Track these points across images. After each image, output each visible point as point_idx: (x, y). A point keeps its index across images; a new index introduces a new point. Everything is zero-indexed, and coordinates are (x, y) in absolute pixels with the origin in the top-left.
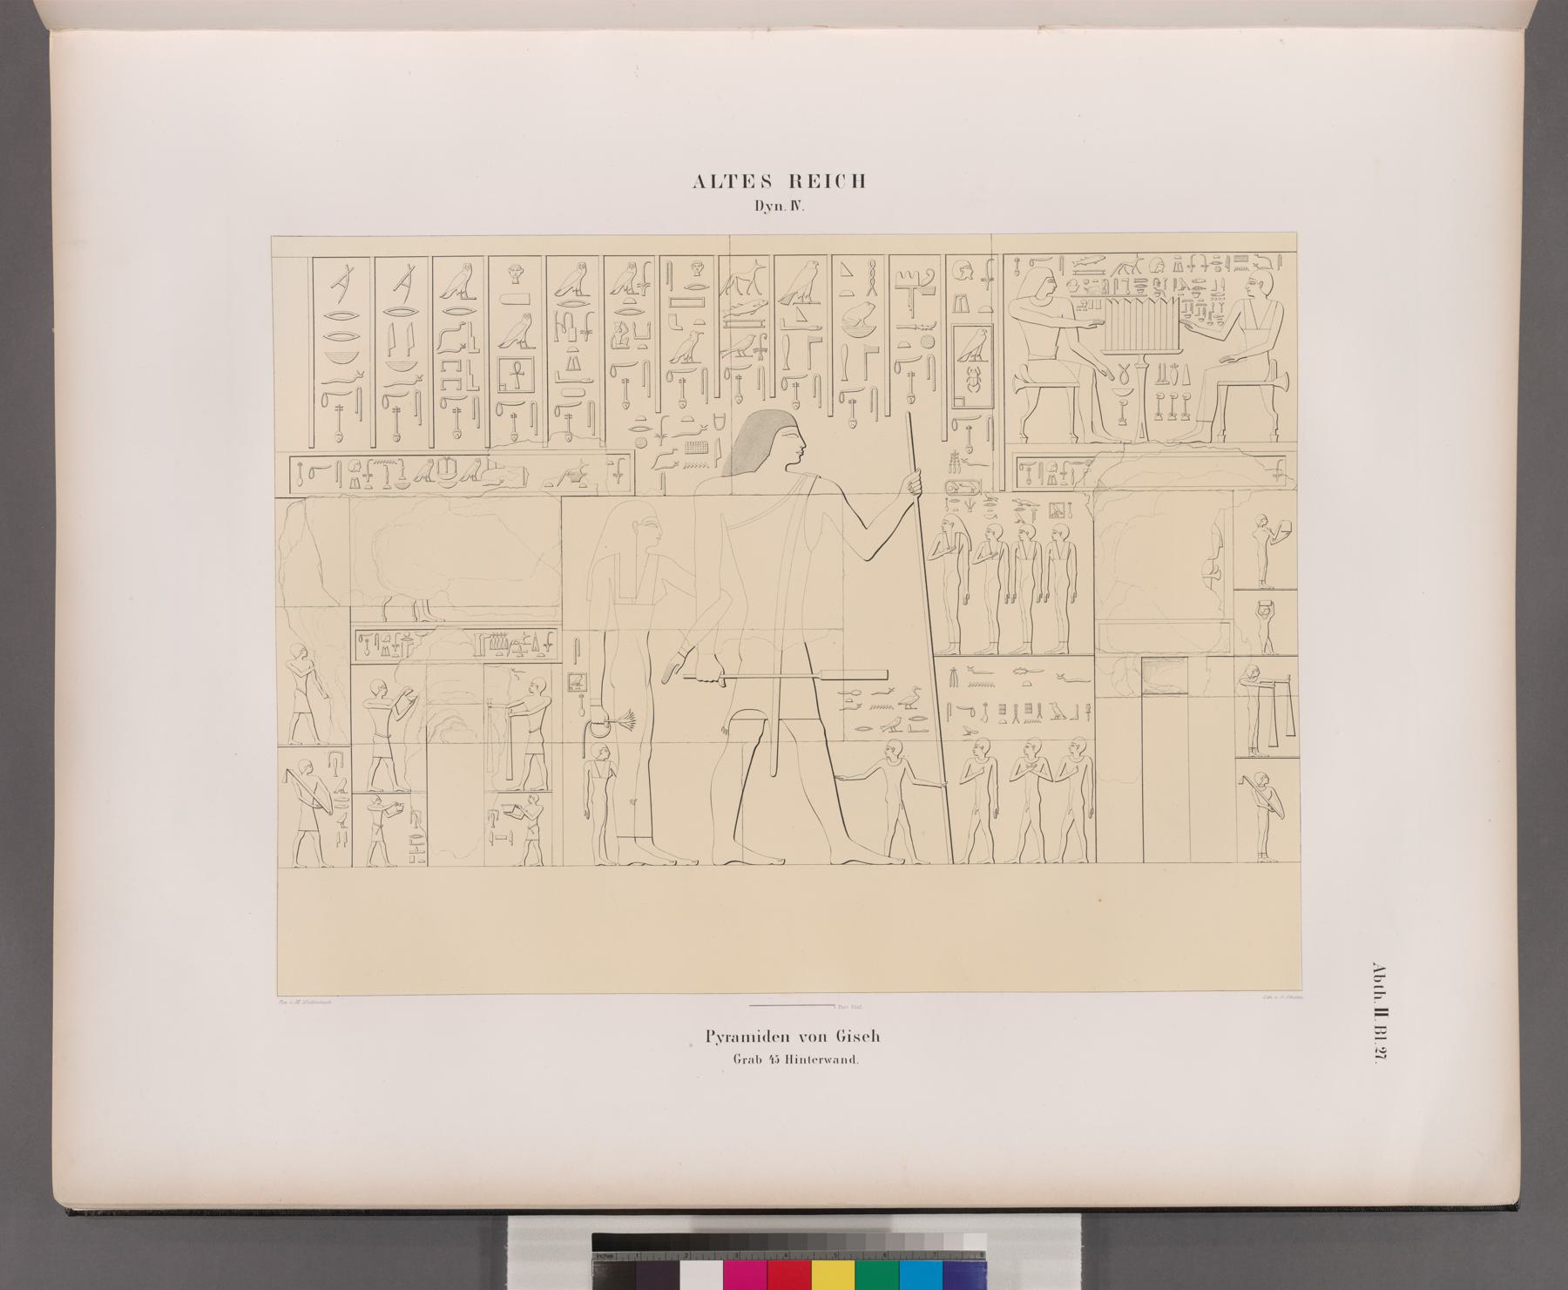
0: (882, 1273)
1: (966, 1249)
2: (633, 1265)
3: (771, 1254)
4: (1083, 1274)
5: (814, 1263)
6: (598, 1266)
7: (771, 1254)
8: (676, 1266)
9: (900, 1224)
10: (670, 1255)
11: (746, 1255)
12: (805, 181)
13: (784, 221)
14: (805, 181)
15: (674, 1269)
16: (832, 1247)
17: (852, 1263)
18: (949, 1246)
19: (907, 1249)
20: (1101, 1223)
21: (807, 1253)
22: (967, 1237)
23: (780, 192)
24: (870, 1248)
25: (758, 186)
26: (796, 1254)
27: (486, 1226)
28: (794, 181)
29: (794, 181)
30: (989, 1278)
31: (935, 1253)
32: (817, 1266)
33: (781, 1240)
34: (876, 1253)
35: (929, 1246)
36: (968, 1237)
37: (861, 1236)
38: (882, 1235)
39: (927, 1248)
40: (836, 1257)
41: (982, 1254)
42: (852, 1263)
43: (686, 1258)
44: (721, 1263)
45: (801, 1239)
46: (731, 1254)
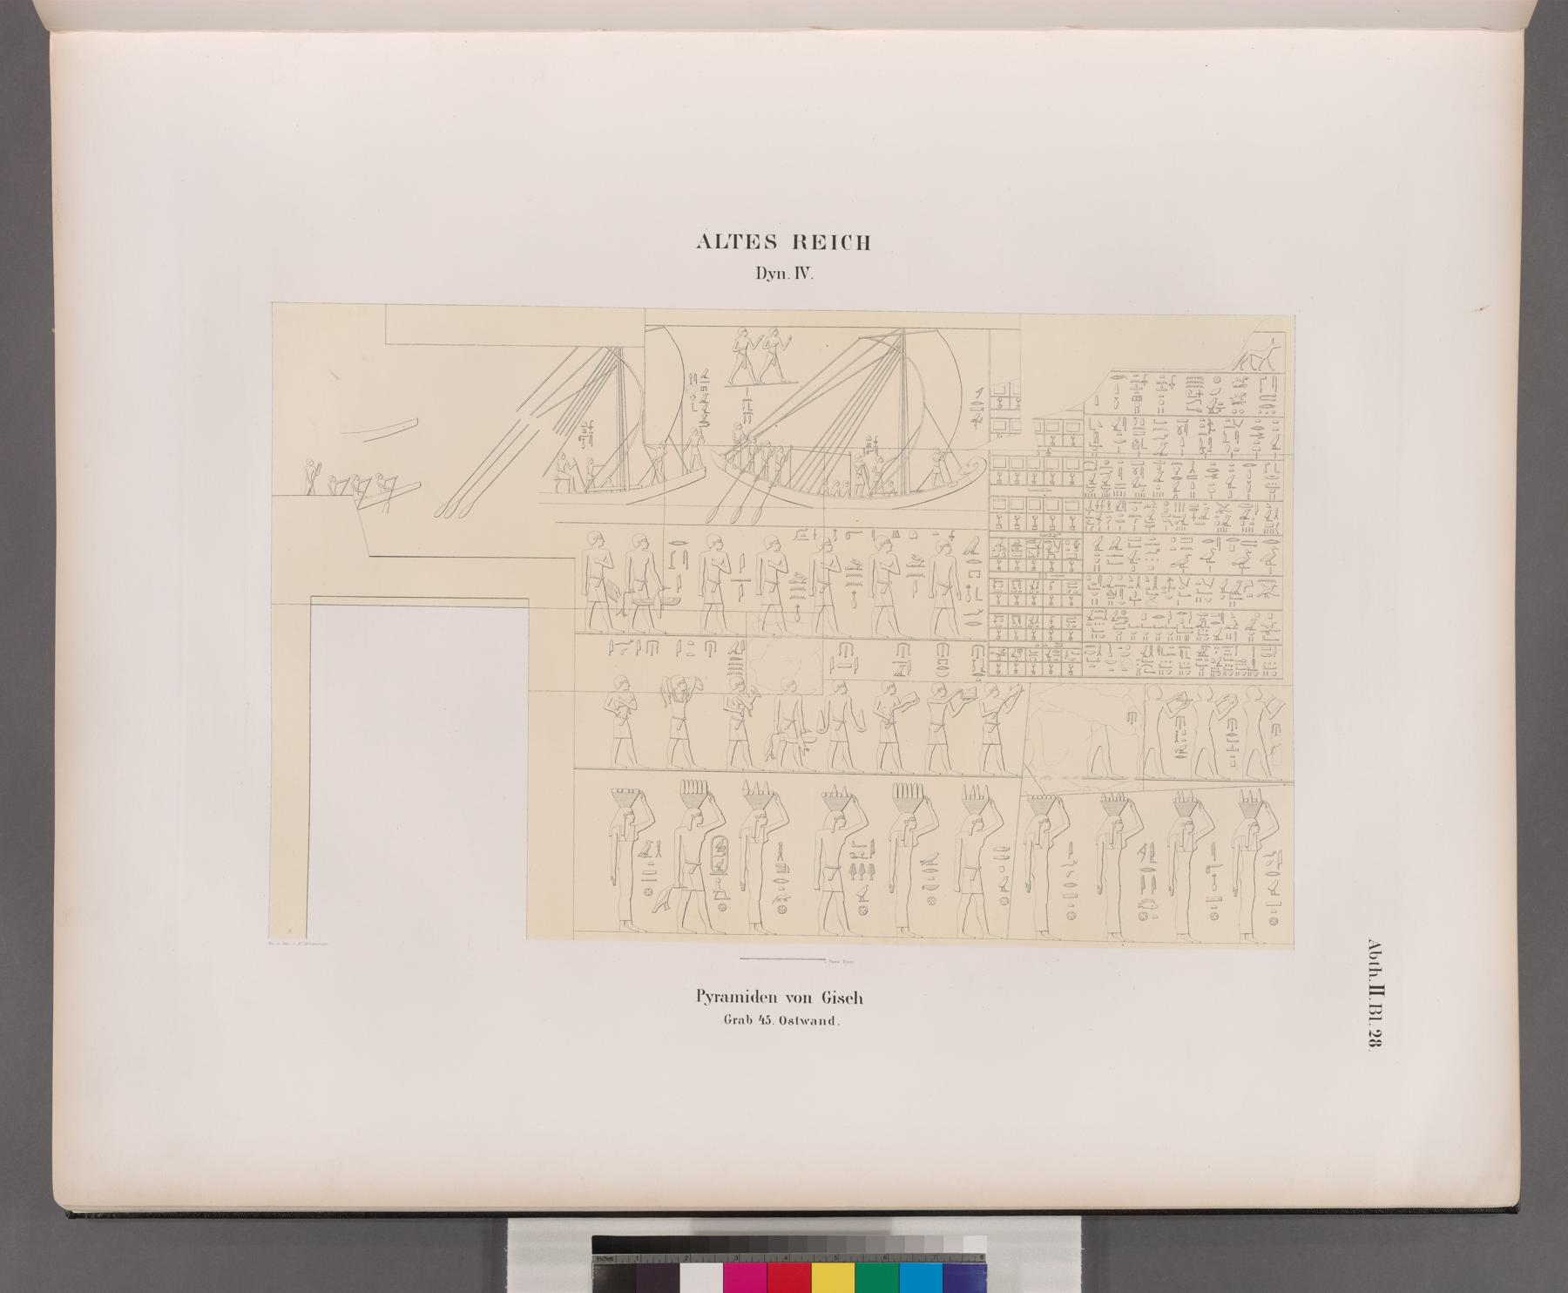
0: (882, 1277)
2: (633, 1267)
4: (1083, 1277)
9: (900, 1226)
10: (669, 1258)
11: (746, 1257)
15: (674, 1271)
16: (832, 1249)
17: (850, 1268)
19: (908, 1250)
20: (1104, 1228)
22: (967, 1239)
24: (871, 1250)
26: (795, 1257)
27: (487, 1228)
30: (989, 1280)
31: (935, 1257)
34: (876, 1256)
36: (968, 1239)
37: (861, 1239)
38: (882, 1237)
39: (928, 1250)
40: (836, 1259)
42: (850, 1268)
45: (801, 1242)
46: (731, 1257)
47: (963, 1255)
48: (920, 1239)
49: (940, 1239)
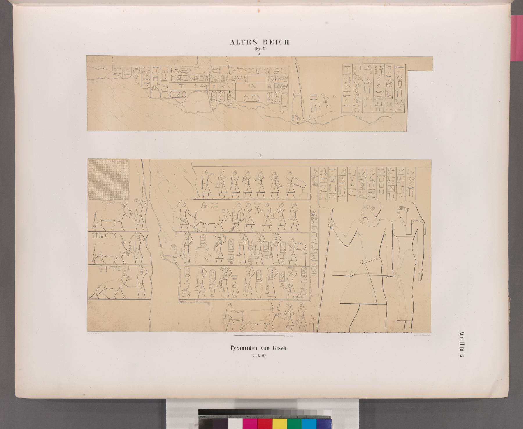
3: (259, 416)
5: (273, 419)
6: (200, 419)
7: (259, 416)
8: (227, 419)
10: (225, 417)
11: (250, 417)
12: (268, 42)
13: (263, 53)
14: (268, 42)
17: (285, 420)
18: (319, 414)
19: (305, 415)
21: (271, 416)
23: (260, 45)
24: (292, 414)
25: (252, 44)
26: (267, 417)
28: (265, 42)
29: (265, 42)
32: (274, 420)
34: (294, 416)
35: (311, 415)
37: (289, 411)
38: (296, 410)
40: (281, 417)
41: (330, 417)
42: (285, 420)
43: (230, 418)
44: (241, 419)
46: (245, 416)
48: (309, 411)
49: (316, 411)
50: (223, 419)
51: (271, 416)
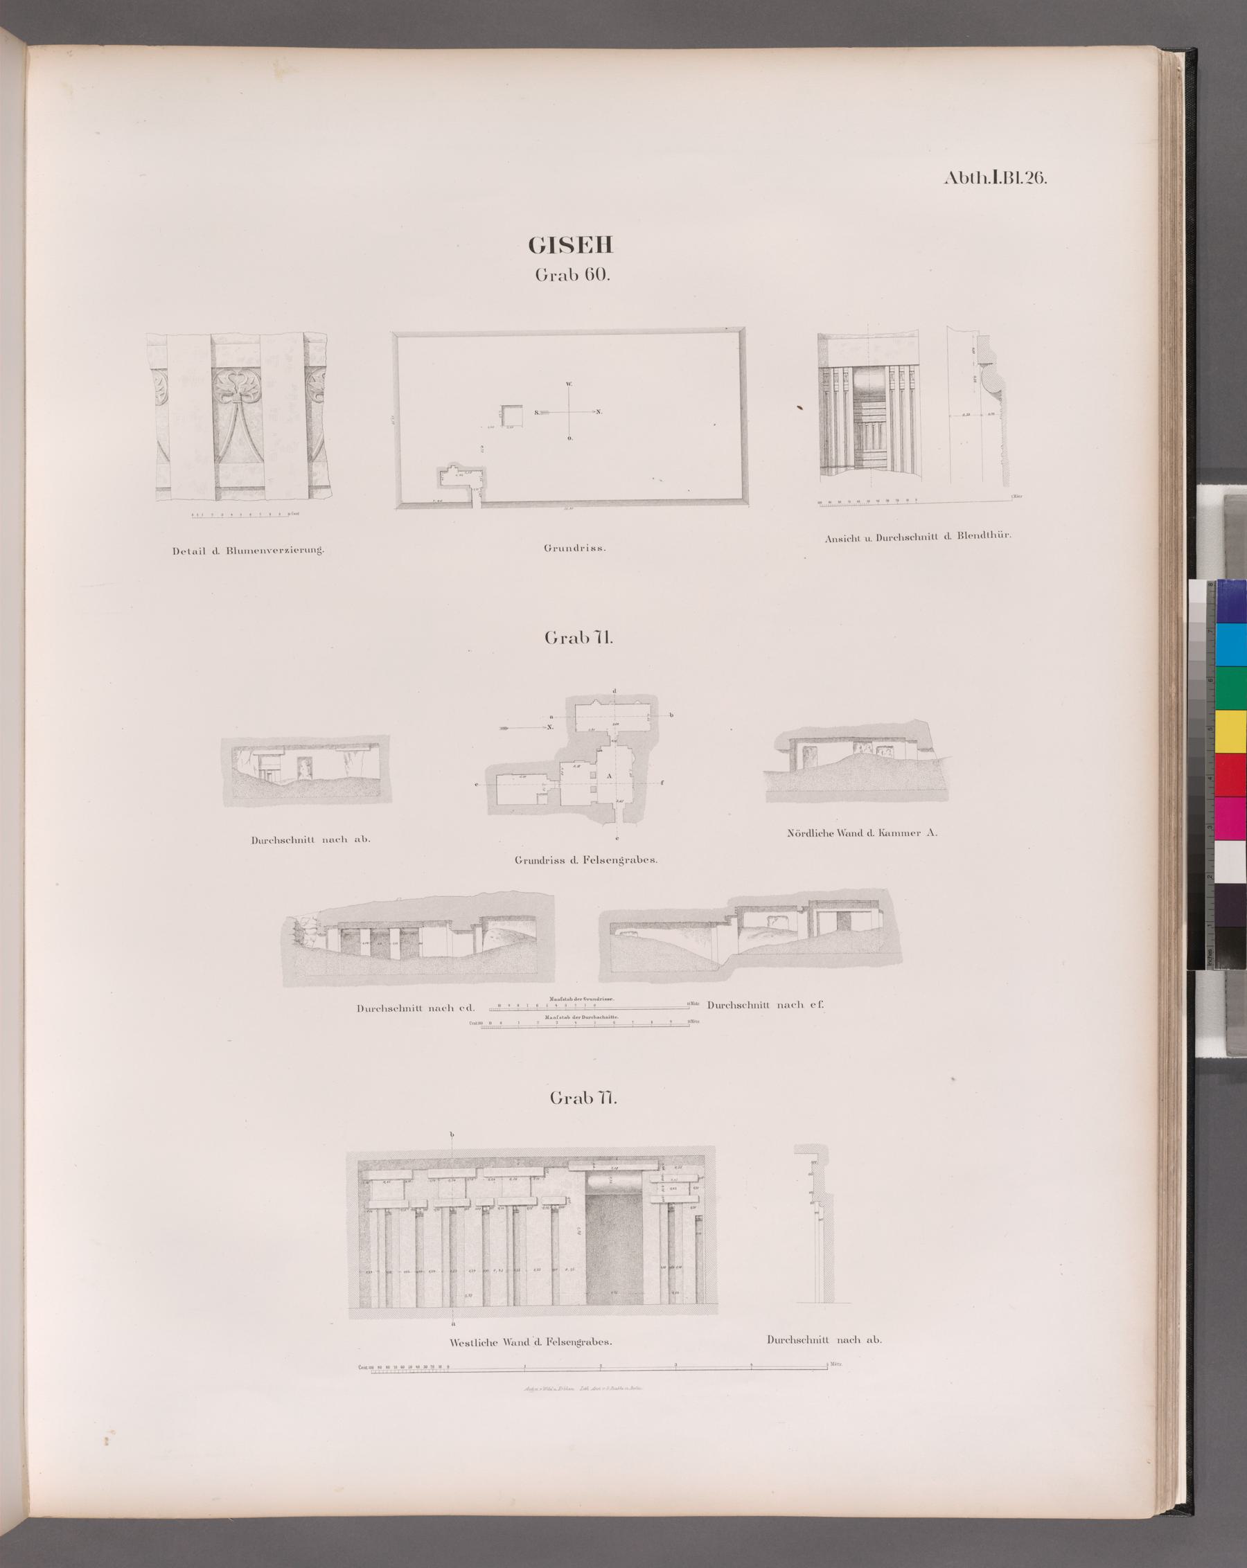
1: (1204, 601)
3: (1209, 794)
5: (1217, 751)
7: (1209, 794)
8: (1221, 887)
10: (1209, 893)
11: (1209, 818)
15: (1226, 890)
16: (1201, 734)
17: (1220, 715)
18: (1204, 621)
19: (1204, 659)
21: (1208, 759)
24: (1202, 694)
26: (1209, 769)
31: (1210, 630)
32: (1220, 748)
33: (1195, 783)
34: (1209, 689)
39: (1204, 639)
40: (1212, 729)
42: (1220, 715)
45: (1195, 763)
46: (1209, 832)
47: (1208, 604)
50: (1216, 897)
51: (1208, 759)
